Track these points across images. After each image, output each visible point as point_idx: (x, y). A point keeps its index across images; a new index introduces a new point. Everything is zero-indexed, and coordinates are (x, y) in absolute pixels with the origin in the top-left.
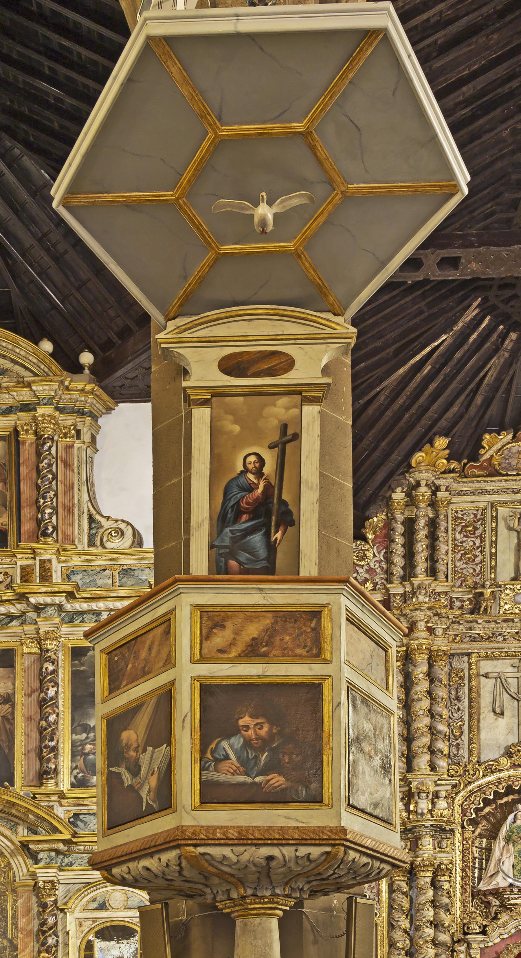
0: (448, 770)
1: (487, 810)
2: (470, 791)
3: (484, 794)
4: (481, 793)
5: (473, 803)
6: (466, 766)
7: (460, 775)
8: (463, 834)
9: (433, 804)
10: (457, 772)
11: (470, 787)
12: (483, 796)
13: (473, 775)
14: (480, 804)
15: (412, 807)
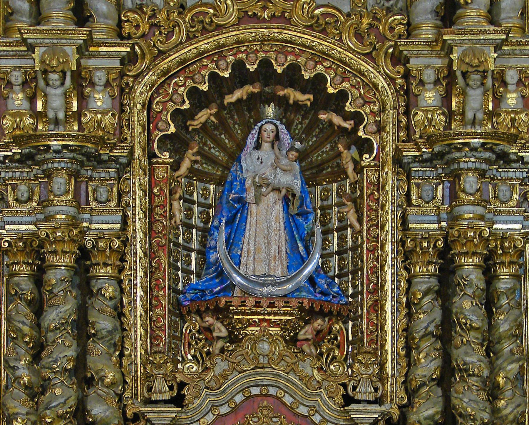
0: (120, 24)
1: (203, 116)
2: (164, 73)
3: (192, 78)
4: (186, 78)
5: (171, 100)
6: (153, 16)
7: (143, 36)
8: (150, 172)
9: (83, 99)
10: (138, 27)
11: (164, 65)
12: (189, 83)
13: (169, 36)
14: (184, 102)
15: (40, 107)
